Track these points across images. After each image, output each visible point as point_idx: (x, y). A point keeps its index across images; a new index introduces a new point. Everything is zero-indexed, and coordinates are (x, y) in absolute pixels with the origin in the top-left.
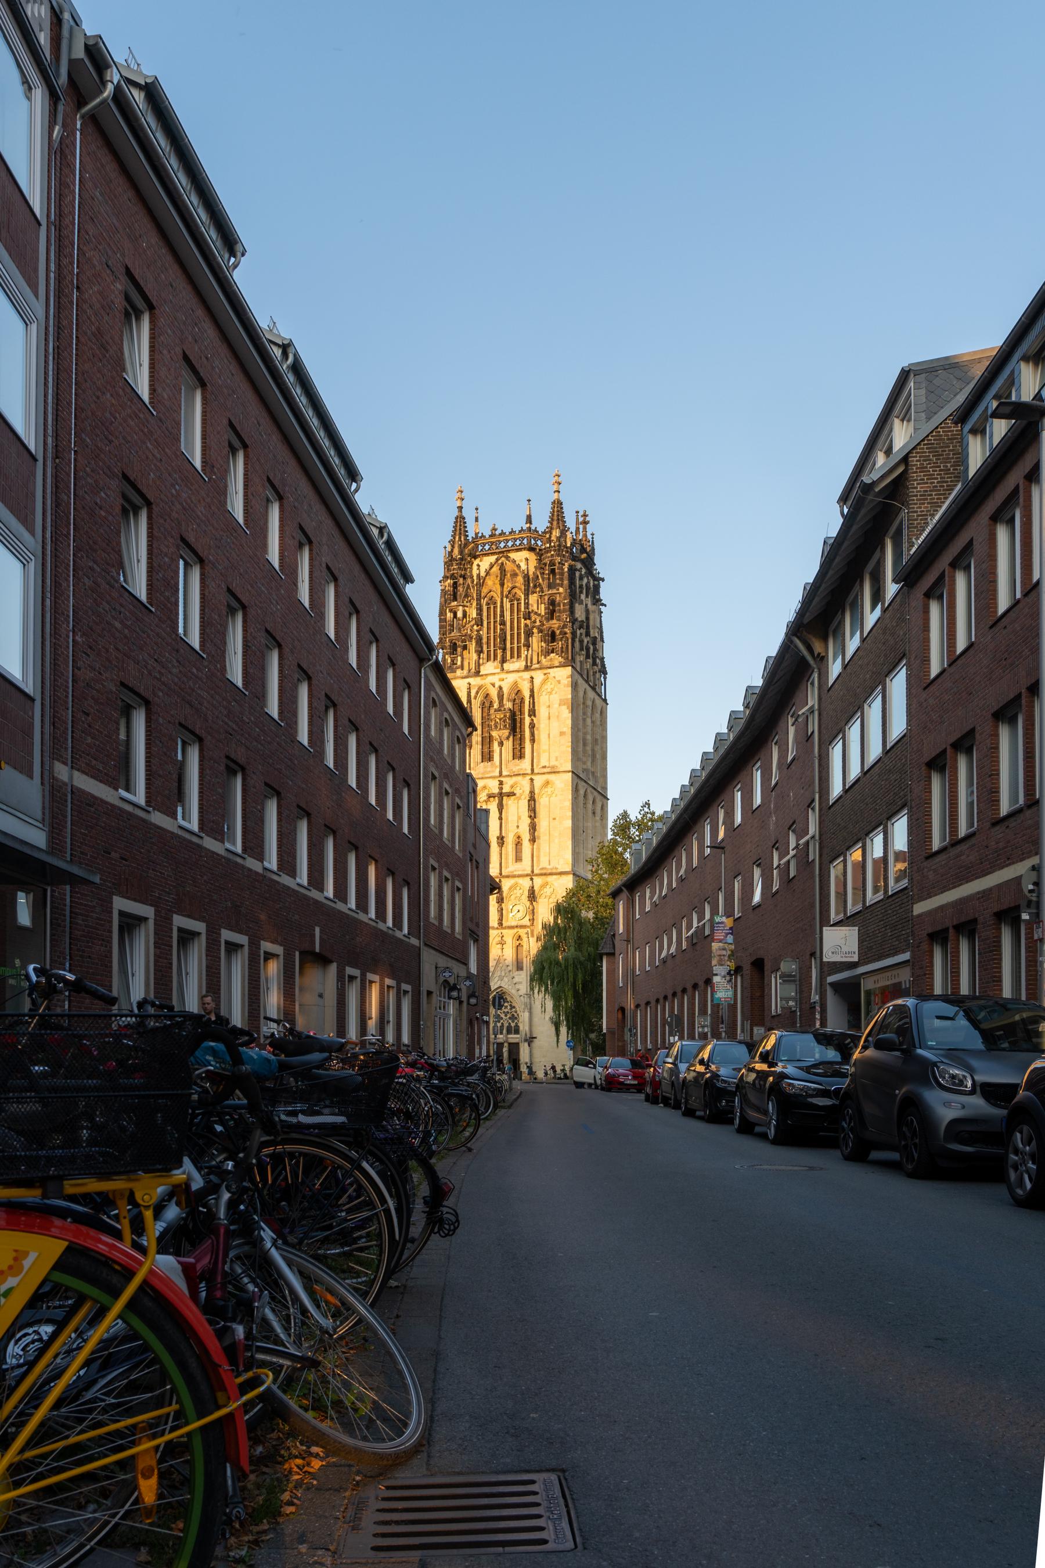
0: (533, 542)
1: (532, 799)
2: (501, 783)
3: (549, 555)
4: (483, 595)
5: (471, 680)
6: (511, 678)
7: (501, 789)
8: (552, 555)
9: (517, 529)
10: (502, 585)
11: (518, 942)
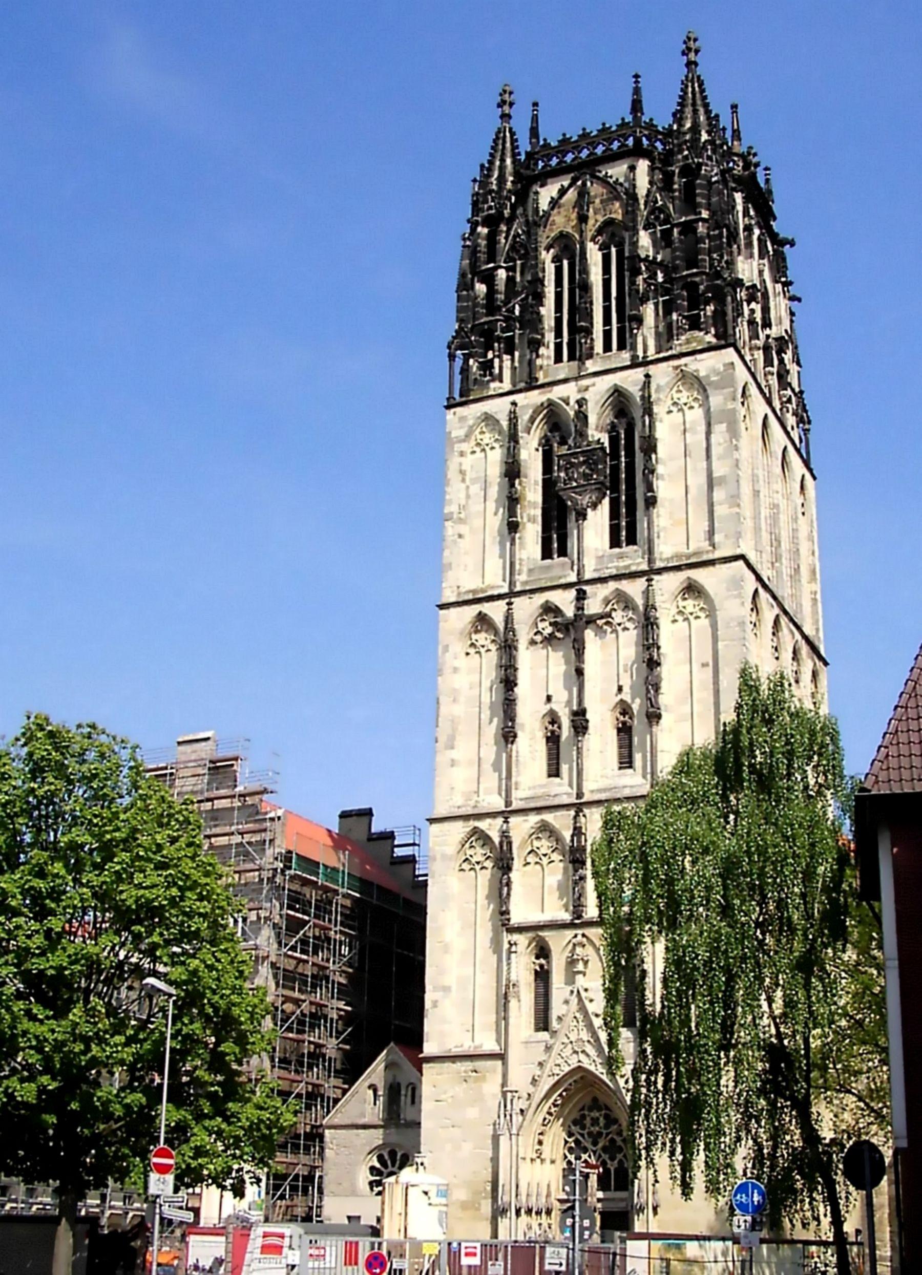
0: (645, 141)
2: (581, 596)
3: (680, 157)
4: (544, 242)
7: (580, 608)
8: (686, 157)
9: (613, 123)
10: (583, 219)
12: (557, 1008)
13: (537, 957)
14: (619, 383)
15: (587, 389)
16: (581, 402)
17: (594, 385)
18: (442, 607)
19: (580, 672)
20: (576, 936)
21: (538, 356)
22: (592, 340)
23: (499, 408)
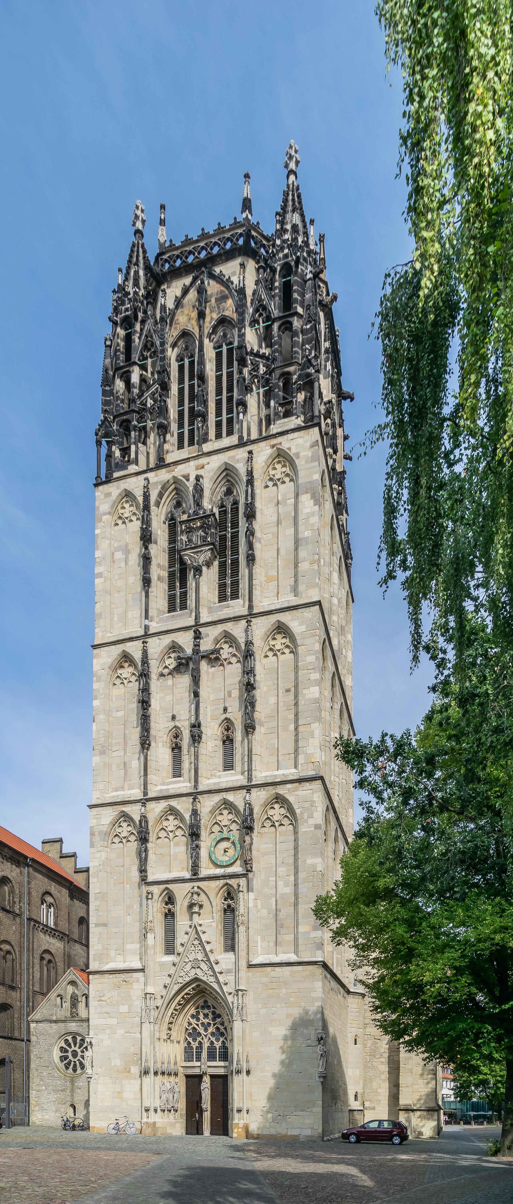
1: (248, 655)
2: (198, 636)
5: (150, 475)
6: (215, 463)
7: (197, 645)
11: (226, 902)
12: (181, 938)
13: (167, 904)
14: (226, 461)
15: (203, 467)
16: (198, 478)
17: (208, 463)
18: (95, 647)
19: (196, 695)
20: (193, 888)
21: (165, 441)
22: (207, 426)
23: (135, 485)
